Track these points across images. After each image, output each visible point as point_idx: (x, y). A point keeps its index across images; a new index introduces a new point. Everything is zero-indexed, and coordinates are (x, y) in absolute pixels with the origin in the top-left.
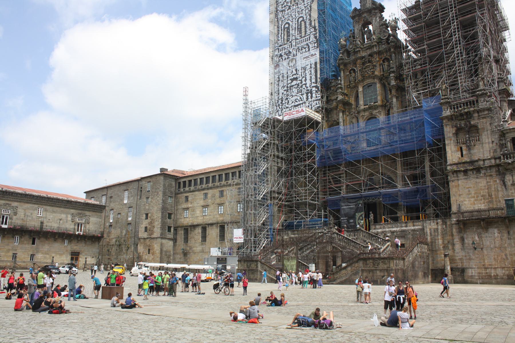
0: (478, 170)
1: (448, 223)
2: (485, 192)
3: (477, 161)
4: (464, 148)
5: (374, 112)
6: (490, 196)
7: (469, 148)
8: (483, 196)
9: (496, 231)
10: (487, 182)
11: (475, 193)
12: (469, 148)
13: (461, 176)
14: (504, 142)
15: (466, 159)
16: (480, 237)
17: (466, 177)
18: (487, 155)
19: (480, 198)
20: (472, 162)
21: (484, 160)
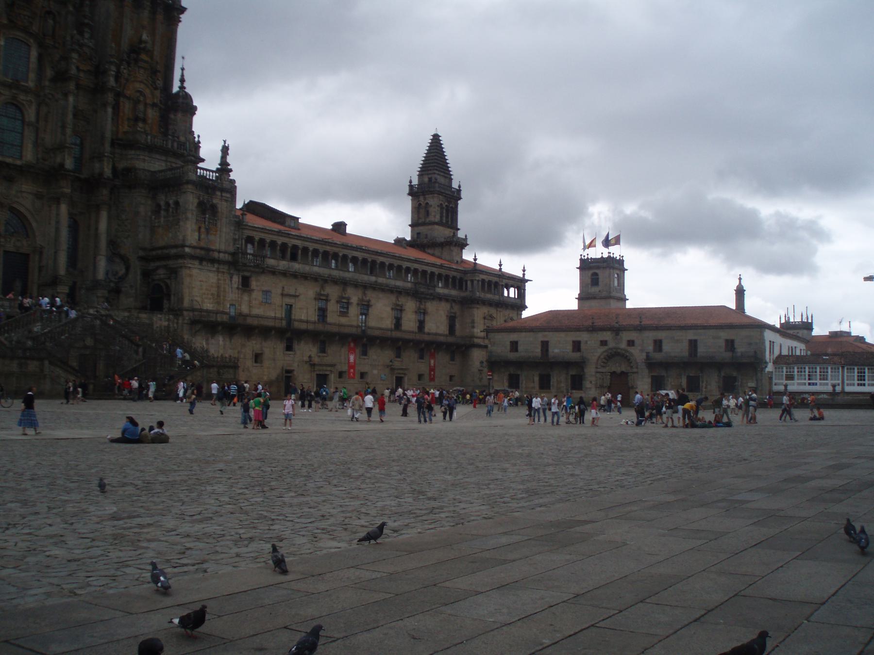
0: (213, 261)
1: (180, 321)
2: (214, 290)
3: (213, 251)
4: (203, 230)
5: (22, 97)
6: (218, 296)
7: (208, 231)
8: (212, 294)
9: (221, 339)
10: (219, 280)
11: (207, 289)
12: (208, 231)
13: (196, 262)
14: (237, 237)
15: (202, 244)
16: (207, 344)
17: (200, 267)
18: (223, 248)
19: (210, 296)
20: (208, 250)
21: (219, 252)
